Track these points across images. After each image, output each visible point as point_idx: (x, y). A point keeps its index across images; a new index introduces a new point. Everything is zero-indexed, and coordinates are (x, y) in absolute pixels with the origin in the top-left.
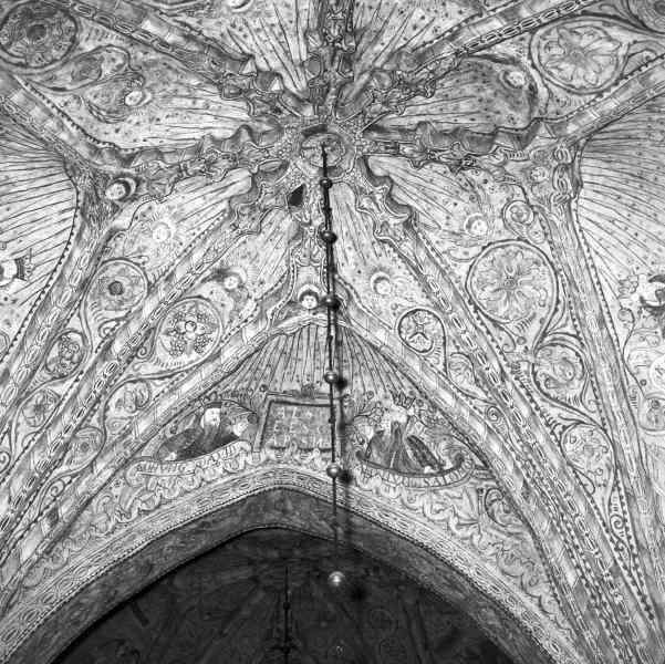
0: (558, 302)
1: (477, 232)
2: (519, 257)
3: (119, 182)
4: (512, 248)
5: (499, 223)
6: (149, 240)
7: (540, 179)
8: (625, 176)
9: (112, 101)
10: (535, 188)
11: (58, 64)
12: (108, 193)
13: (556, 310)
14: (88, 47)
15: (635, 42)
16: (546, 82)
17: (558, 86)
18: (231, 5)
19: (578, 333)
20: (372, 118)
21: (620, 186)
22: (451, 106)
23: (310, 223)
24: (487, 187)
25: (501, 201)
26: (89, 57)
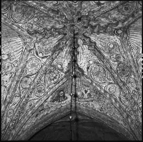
0: (12, 18)
1: (36, 19)
2: (25, 19)
3: (118, 34)
4: (27, 20)
5: (32, 23)
6: (115, 16)
7: (29, 39)
8: (11, 41)
9: (115, 48)
10: (29, 37)
11: (122, 63)
12: (121, 32)
13: (11, 16)
14: (116, 63)
15: (26, 74)
16: (36, 57)
17: (34, 58)
18: (91, 61)
19: (3, 15)
20: (65, 39)
21: (11, 38)
22: (50, 42)
23: (76, 16)
24: (37, 28)
25: (33, 27)
26: (117, 61)
